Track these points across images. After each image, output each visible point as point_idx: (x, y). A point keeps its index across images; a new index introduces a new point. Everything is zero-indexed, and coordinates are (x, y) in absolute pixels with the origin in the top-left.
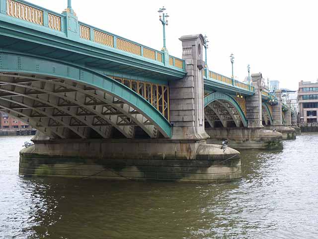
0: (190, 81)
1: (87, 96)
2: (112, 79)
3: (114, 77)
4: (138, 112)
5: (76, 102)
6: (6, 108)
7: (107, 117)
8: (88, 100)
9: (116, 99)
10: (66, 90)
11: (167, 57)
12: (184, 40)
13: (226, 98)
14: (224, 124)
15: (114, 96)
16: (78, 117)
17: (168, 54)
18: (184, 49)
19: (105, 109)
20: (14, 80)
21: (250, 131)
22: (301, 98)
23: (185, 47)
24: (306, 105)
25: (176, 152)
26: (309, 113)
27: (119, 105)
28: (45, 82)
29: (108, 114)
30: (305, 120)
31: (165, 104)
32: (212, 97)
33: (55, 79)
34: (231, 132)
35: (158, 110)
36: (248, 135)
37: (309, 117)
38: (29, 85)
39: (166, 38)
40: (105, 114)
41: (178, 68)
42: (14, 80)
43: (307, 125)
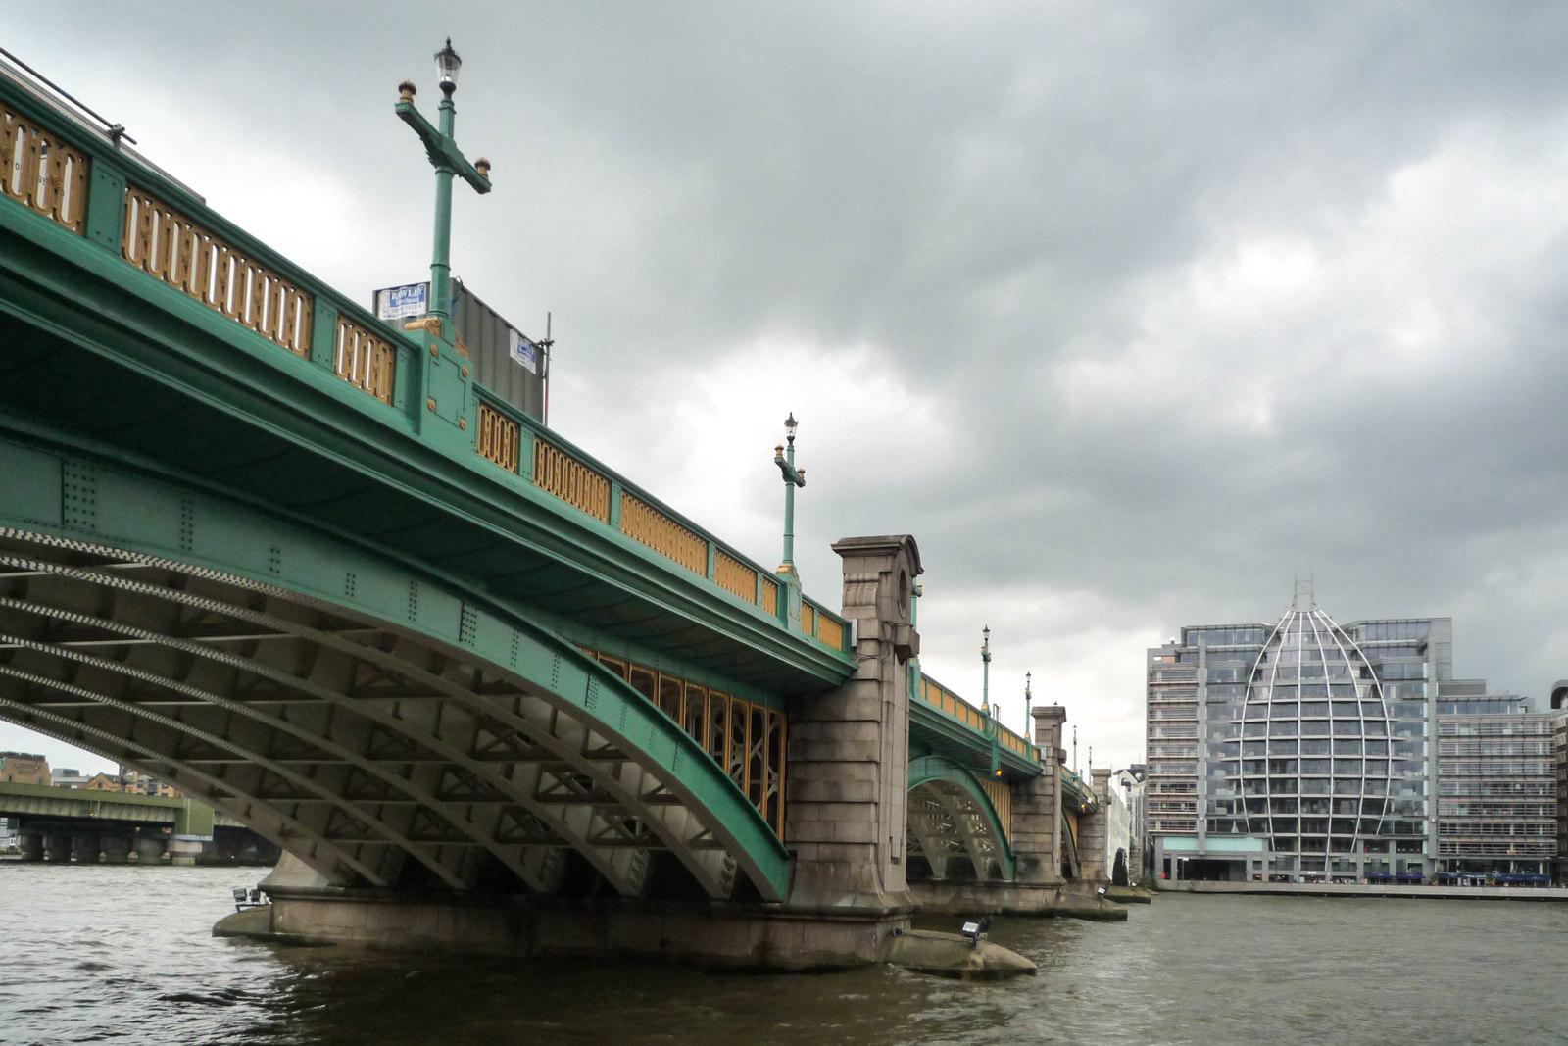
0: (864, 700)
1: (485, 722)
2: (588, 655)
4: (678, 796)
6: (158, 758)
8: (486, 738)
9: (597, 741)
10: (401, 688)
11: (794, 603)
12: (849, 550)
15: (590, 723)
16: (442, 808)
17: (799, 590)
18: (848, 582)
19: (549, 780)
23: (854, 577)
27: (605, 766)
32: (935, 770)
35: (746, 793)
39: (795, 532)
40: (546, 798)
41: (828, 641)
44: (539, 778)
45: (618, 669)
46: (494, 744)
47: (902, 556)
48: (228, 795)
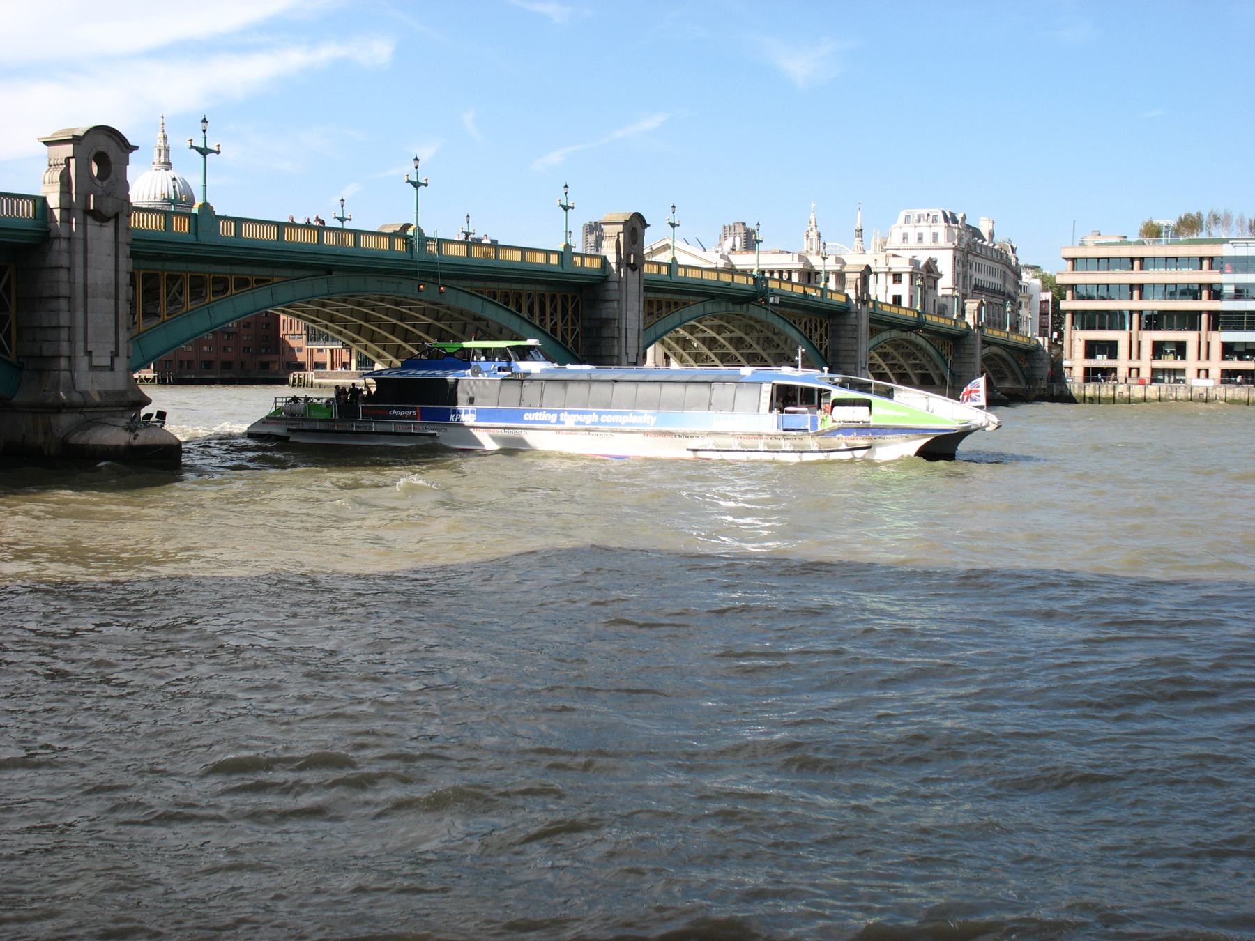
26: (1092, 349)
30: (1078, 373)
37: (1092, 363)
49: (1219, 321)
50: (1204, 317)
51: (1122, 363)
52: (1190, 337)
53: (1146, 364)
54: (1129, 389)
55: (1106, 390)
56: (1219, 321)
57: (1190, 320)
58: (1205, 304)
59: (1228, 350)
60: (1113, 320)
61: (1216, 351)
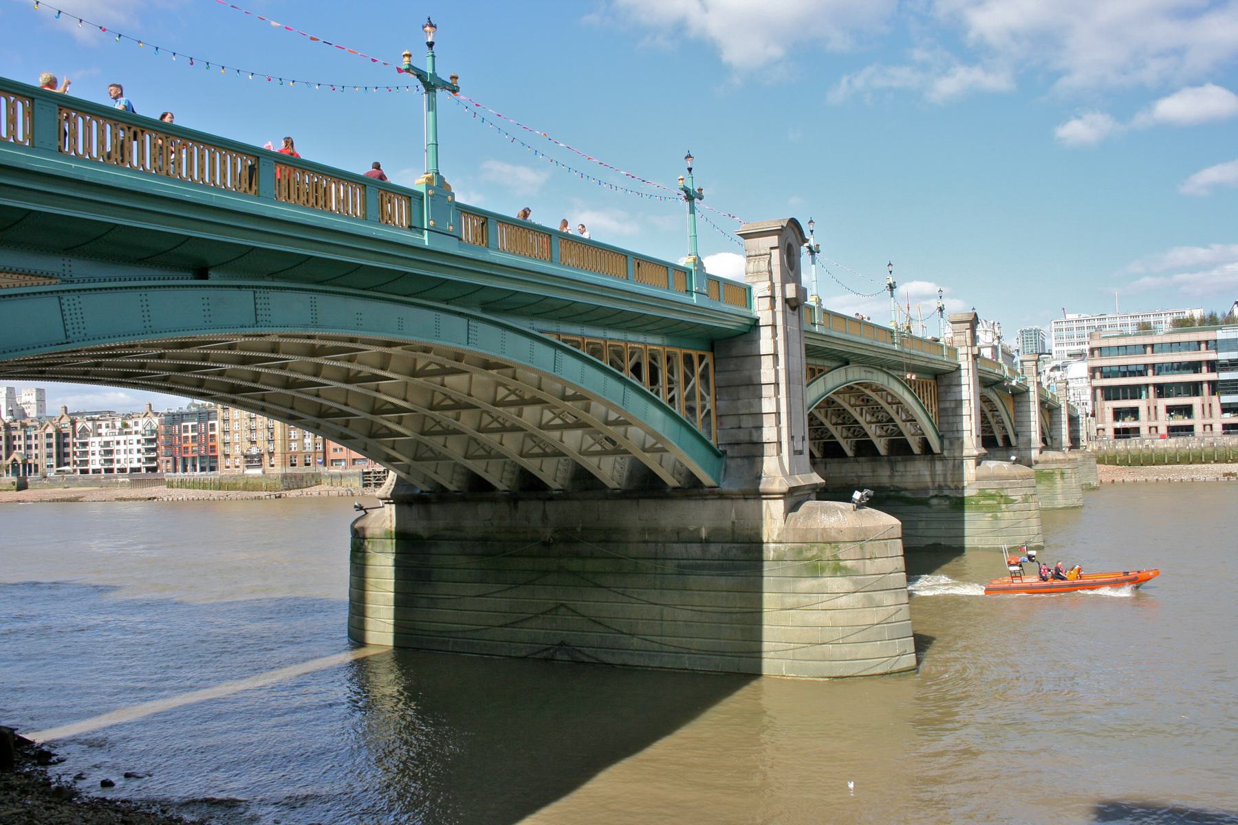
2: (553, 339)
3: (558, 336)
5: (473, 401)
7: (556, 435)
8: (502, 392)
13: (879, 379)
14: (881, 446)
19: (548, 415)
20: (314, 352)
21: (951, 463)
22: (1098, 375)
24: (1110, 393)
25: (733, 523)
26: (1118, 414)
28: (390, 355)
29: (557, 427)
30: (1110, 433)
31: (703, 398)
33: (405, 344)
34: (900, 467)
36: (945, 475)
37: (1119, 425)
38: (350, 360)
42: (314, 352)
43: (1114, 443)
44: (542, 413)
45: (578, 345)
46: (508, 396)
47: (789, 231)
48: (354, 438)
49: (1215, 387)
50: (1205, 386)
51: (1143, 423)
52: (1195, 401)
53: (1164, 421)
54: (1153, 442)
55: (1132, 444)
56: (1215, 387)
57: (1194, 389)
58: (1205, 376)
59: (1226, 409)
60: (1135, 391)
61: (1217, 409)
